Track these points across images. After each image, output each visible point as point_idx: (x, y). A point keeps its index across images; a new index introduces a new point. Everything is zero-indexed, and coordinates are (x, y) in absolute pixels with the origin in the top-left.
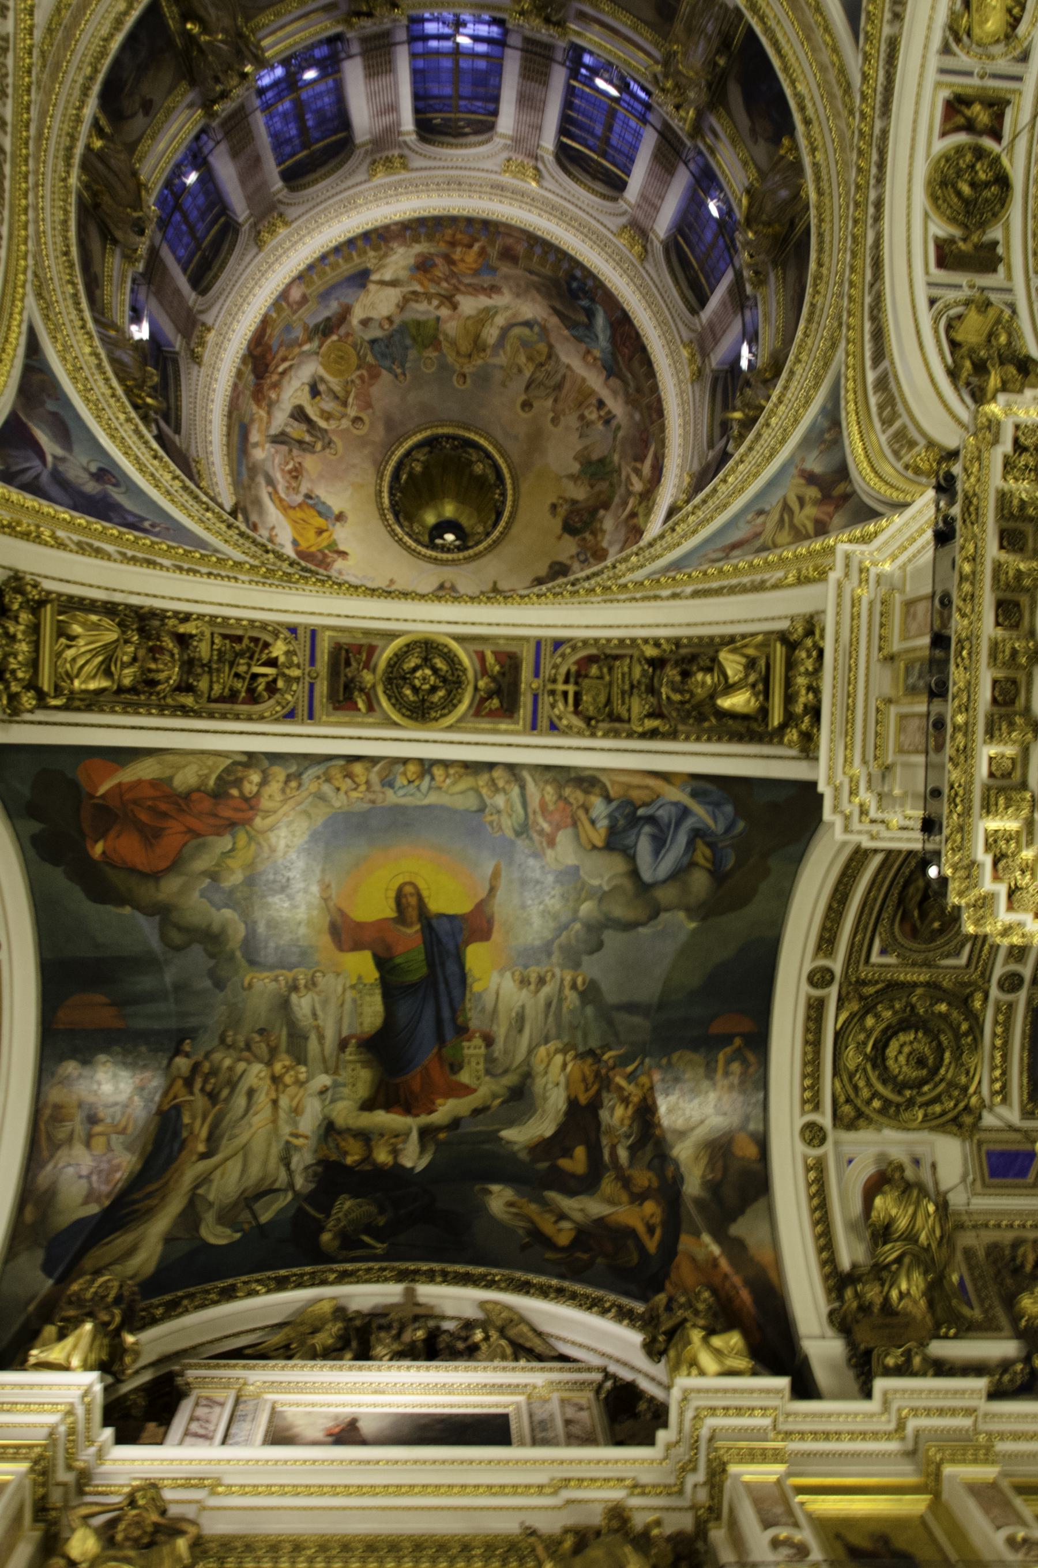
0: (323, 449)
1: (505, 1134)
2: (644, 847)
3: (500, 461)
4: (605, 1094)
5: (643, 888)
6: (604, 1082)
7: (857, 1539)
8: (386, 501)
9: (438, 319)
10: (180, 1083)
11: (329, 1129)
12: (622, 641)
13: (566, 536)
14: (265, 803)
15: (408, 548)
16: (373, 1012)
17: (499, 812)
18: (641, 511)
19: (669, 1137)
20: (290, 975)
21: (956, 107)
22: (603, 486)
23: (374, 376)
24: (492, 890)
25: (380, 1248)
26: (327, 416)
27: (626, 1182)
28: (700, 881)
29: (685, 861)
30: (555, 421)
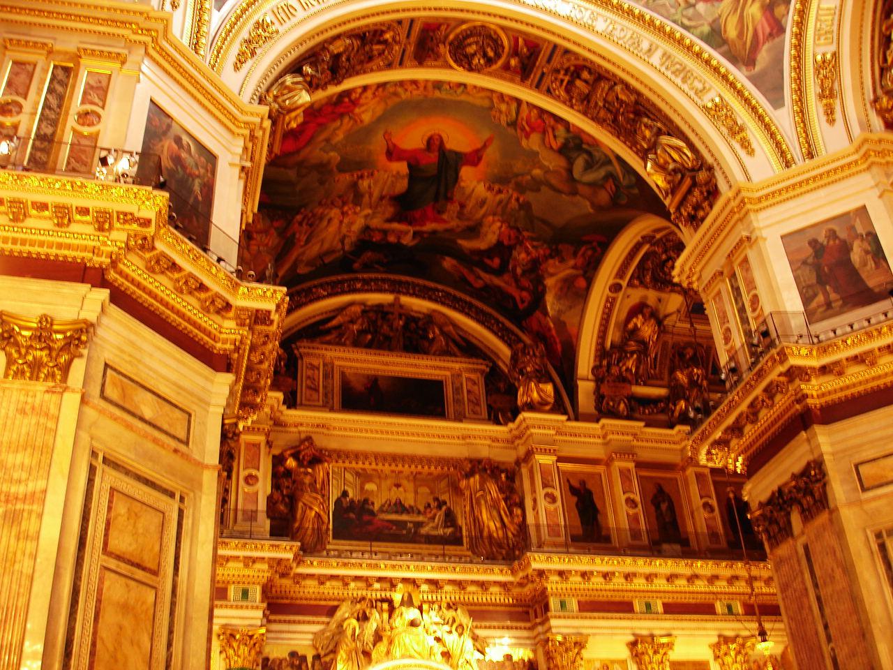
1: (460, 242)
2: (579, 163)
4: (518, 247)
5: (571, 178)
6: (520, 242)
10: (297, 225)
11: (367, 228)
14: (362, 101)
16: (402, 185)
17: (501, 112)
19: (546, 275)
20: (359, 173)
24: (485, 146)
25: (381, 269)
27: (517, 281)
28: (603, 197)
29: (600, 183)
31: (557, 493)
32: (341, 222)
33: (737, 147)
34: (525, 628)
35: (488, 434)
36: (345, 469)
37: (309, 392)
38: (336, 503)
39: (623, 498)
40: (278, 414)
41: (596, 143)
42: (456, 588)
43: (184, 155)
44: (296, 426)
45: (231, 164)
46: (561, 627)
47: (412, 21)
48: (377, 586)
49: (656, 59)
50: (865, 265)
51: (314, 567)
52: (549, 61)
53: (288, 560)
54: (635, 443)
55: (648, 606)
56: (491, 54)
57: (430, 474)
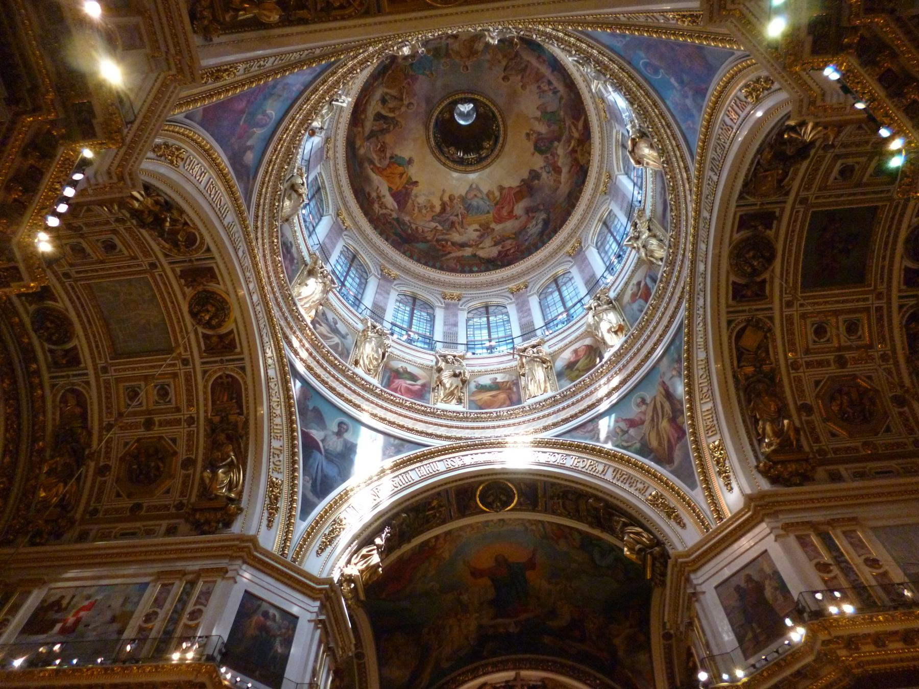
0: (394, 127)
2: (597, 555)
3: (494, 109)
8: (433, 143)
9: (447, 44)
11: (480, 626)
12: (582, 490)
13: (536, 153)
15: (450, 168)
16: (491, 594)
18: (579, 149)
21: (744, 222)
22: (555, 127)
23: (414, 79)
24: (534, 556)
26: (392, 110)
30: (523, 87)
32: (460, 626)
33: (672, 523)
41: (600, 539)
43: (269, 623)
45: (310, 621)
47: (447, 491)
49: (609, 476)
50: (777, 600)
52: (545, 493)
56: (504, 498)
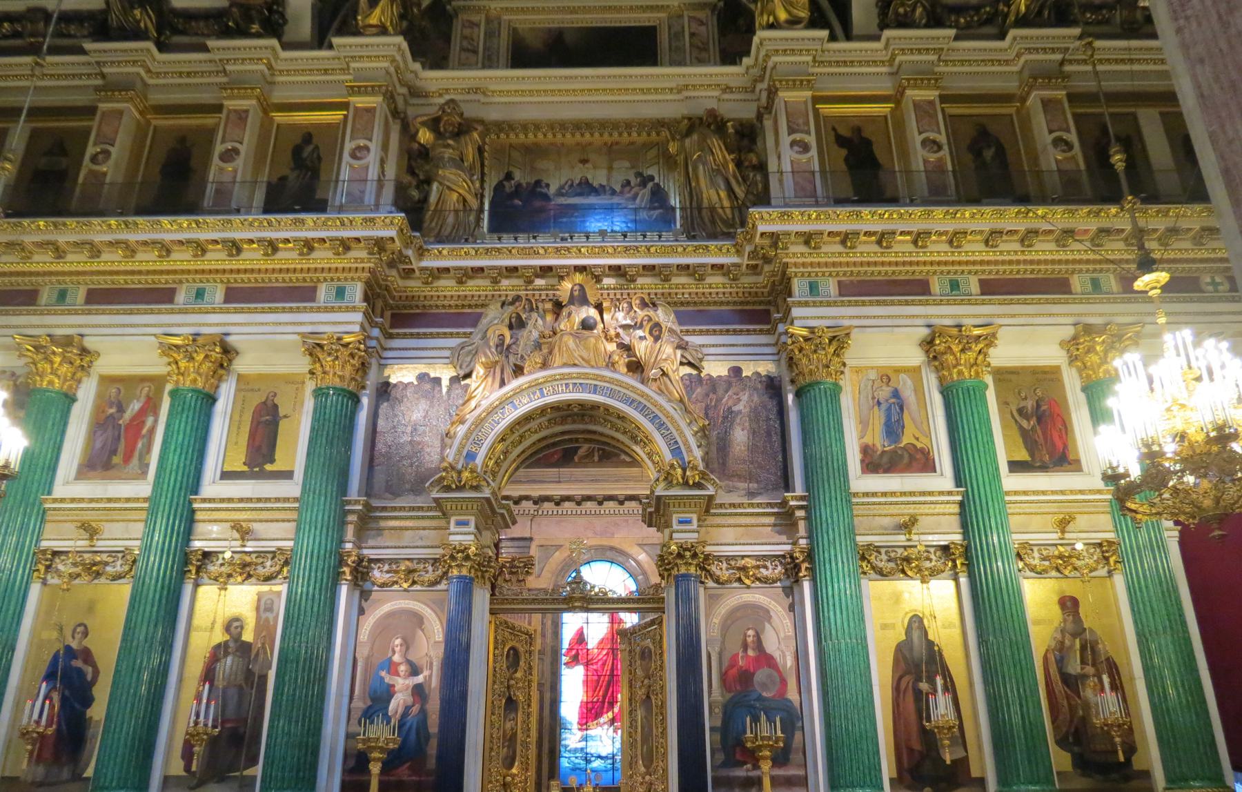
7: (844, 131)
31: (811, 139)
34: (761, 332)
35: (714, 81)
36: (511, 145)
37: (464, 55)
38: (496, 189)
39: (919, 139)
40: (409, 76)
42: (656, 281)
44: (441, 95)
46: (805, 318)
48: (539, 282)
51: (442, 257)
53: (392, 239)
54: (942, 69)
55: (955, 285)
57: (632, 143)
